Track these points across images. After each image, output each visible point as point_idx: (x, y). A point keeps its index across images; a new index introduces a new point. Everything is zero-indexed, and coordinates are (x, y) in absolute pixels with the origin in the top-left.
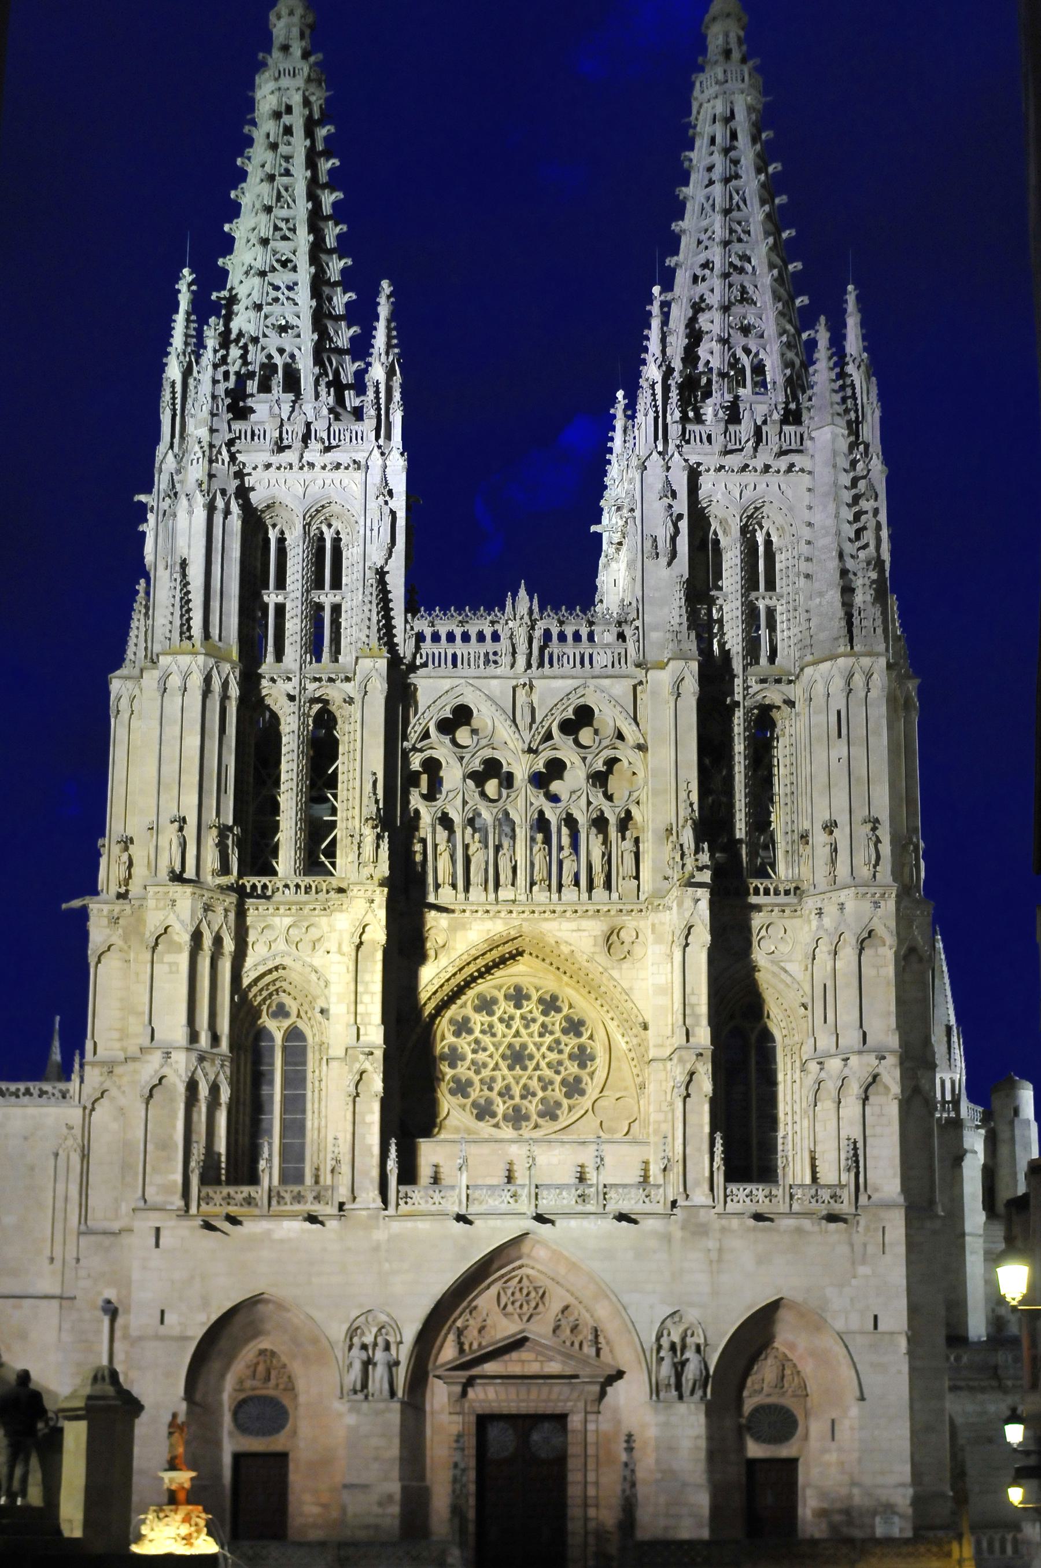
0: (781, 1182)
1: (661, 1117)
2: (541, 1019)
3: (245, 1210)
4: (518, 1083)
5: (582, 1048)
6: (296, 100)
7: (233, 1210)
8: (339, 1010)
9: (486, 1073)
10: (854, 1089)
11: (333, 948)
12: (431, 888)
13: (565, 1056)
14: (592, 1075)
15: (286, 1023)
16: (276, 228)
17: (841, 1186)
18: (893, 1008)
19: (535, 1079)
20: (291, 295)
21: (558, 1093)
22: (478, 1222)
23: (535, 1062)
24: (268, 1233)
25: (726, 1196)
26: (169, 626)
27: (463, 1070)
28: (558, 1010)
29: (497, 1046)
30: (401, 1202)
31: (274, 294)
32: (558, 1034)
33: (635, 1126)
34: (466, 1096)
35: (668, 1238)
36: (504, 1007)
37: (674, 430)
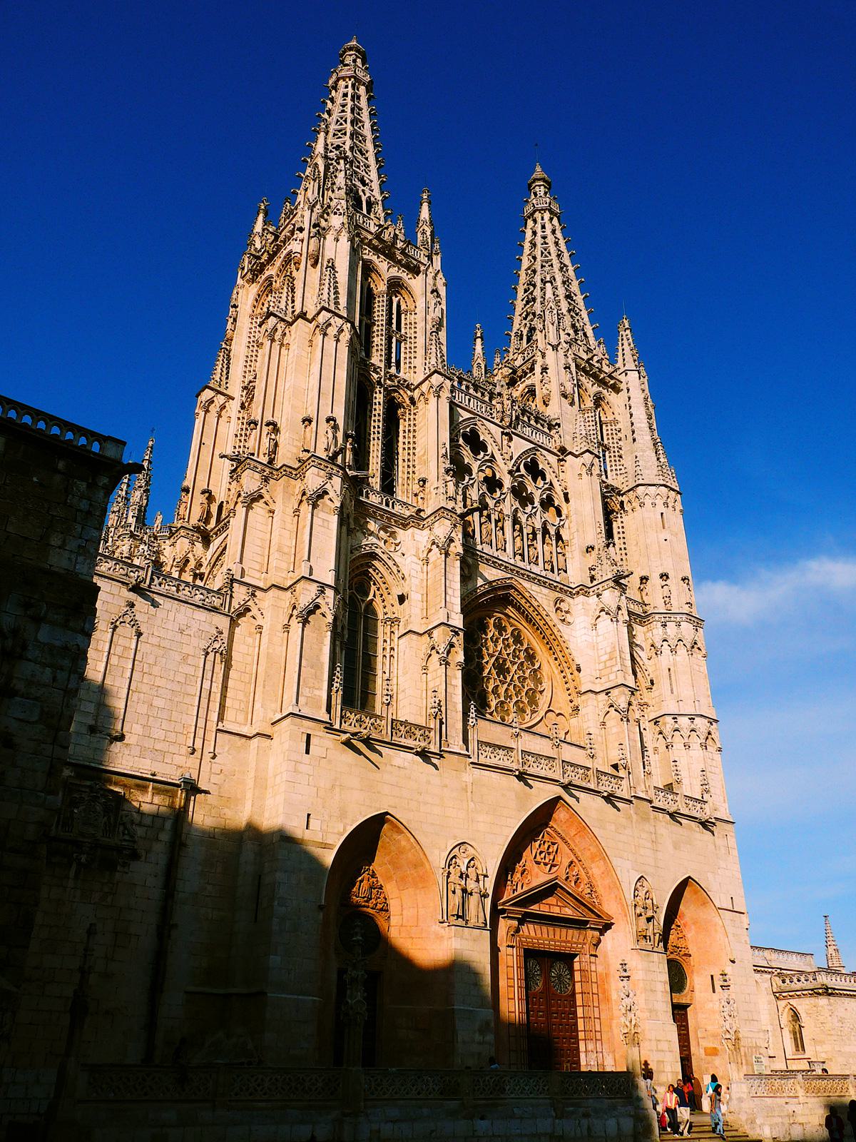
2: (514, 647)
13: (527, 675)
14: (541, 692)
23: (511, 674)
29: (491, 656)
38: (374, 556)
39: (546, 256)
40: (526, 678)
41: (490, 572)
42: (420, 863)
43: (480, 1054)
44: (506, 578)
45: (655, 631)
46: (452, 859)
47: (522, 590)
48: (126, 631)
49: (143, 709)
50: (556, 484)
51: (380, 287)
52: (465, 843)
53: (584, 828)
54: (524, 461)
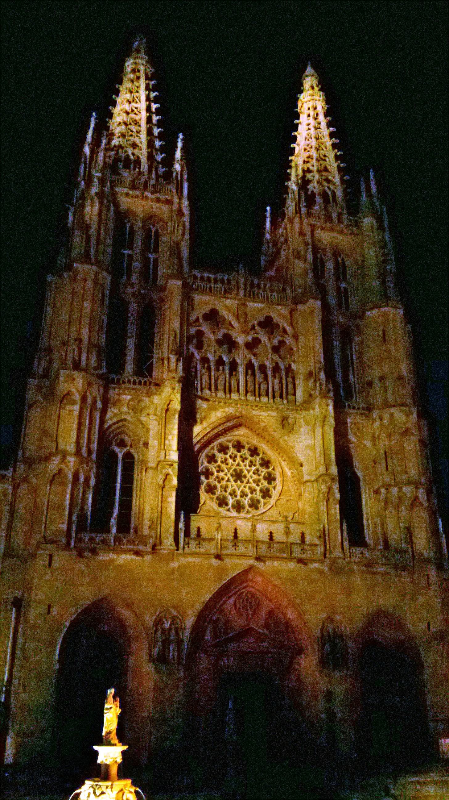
1: (312, 510)
2: (250, 458)
3: (101, 546)
4: (239, 489)
5: (269, 474)
6: (142, 68)
9: (224, 483)
11: (152, 411)
12: (199, 389)
14: (274, 488)
15: (125, 450)
16: (132, 111)
20: (138, 135)
21: (258, 496)
22: (227, 560)
24: (112, 561)
27: (212, 480)
28: (258, 454)
29: (229, 470)
30: (186, 546)
31: (130, 133)
32: (258, 466)
34: (214, 494)
36: (232, 451)
37: (304, 210)
38: (124, 420)
50: (289, 329)
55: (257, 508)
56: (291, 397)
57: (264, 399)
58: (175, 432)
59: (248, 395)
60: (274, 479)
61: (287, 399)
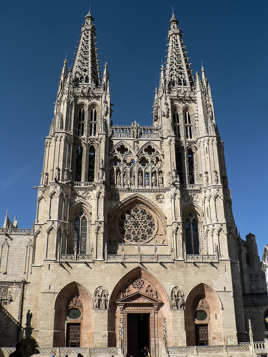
0: (200, 254)
1: (171, 239)
2: (142, 216)
7: (67, 261)
8: (94, 213)
10: (216, 232)
14: (154, 229)
17: (215, 255)
18: (224, 213)
19: (141, 230)
21: (146, 234)
23: (140, 226)
25: (187, 258)
26: (58, 127)
28: (146, 214)
29: (131, 222)
30: (108, 259)
33: (165, 242)
35: (173, 268)
39: (172, 54)
40: (147, 226)
41: (127, 194)
42: (87, 294)
43: (102, 343)
44: (134, 195)
45: (202, 195)
46: (97, 291)
47: (141, 197)
48: (6, 246)
49: (11, 265)
50: (159, 151)
51: (86, 109)
52: (101, 286)
53: (150, 275)
54: (144, 148)
55: (145, 239)
56: (162, 185)
57: (147, 187)
58: (103, 207)
59: (140, 185)
60: (154, 225)
61: (159, 186)
